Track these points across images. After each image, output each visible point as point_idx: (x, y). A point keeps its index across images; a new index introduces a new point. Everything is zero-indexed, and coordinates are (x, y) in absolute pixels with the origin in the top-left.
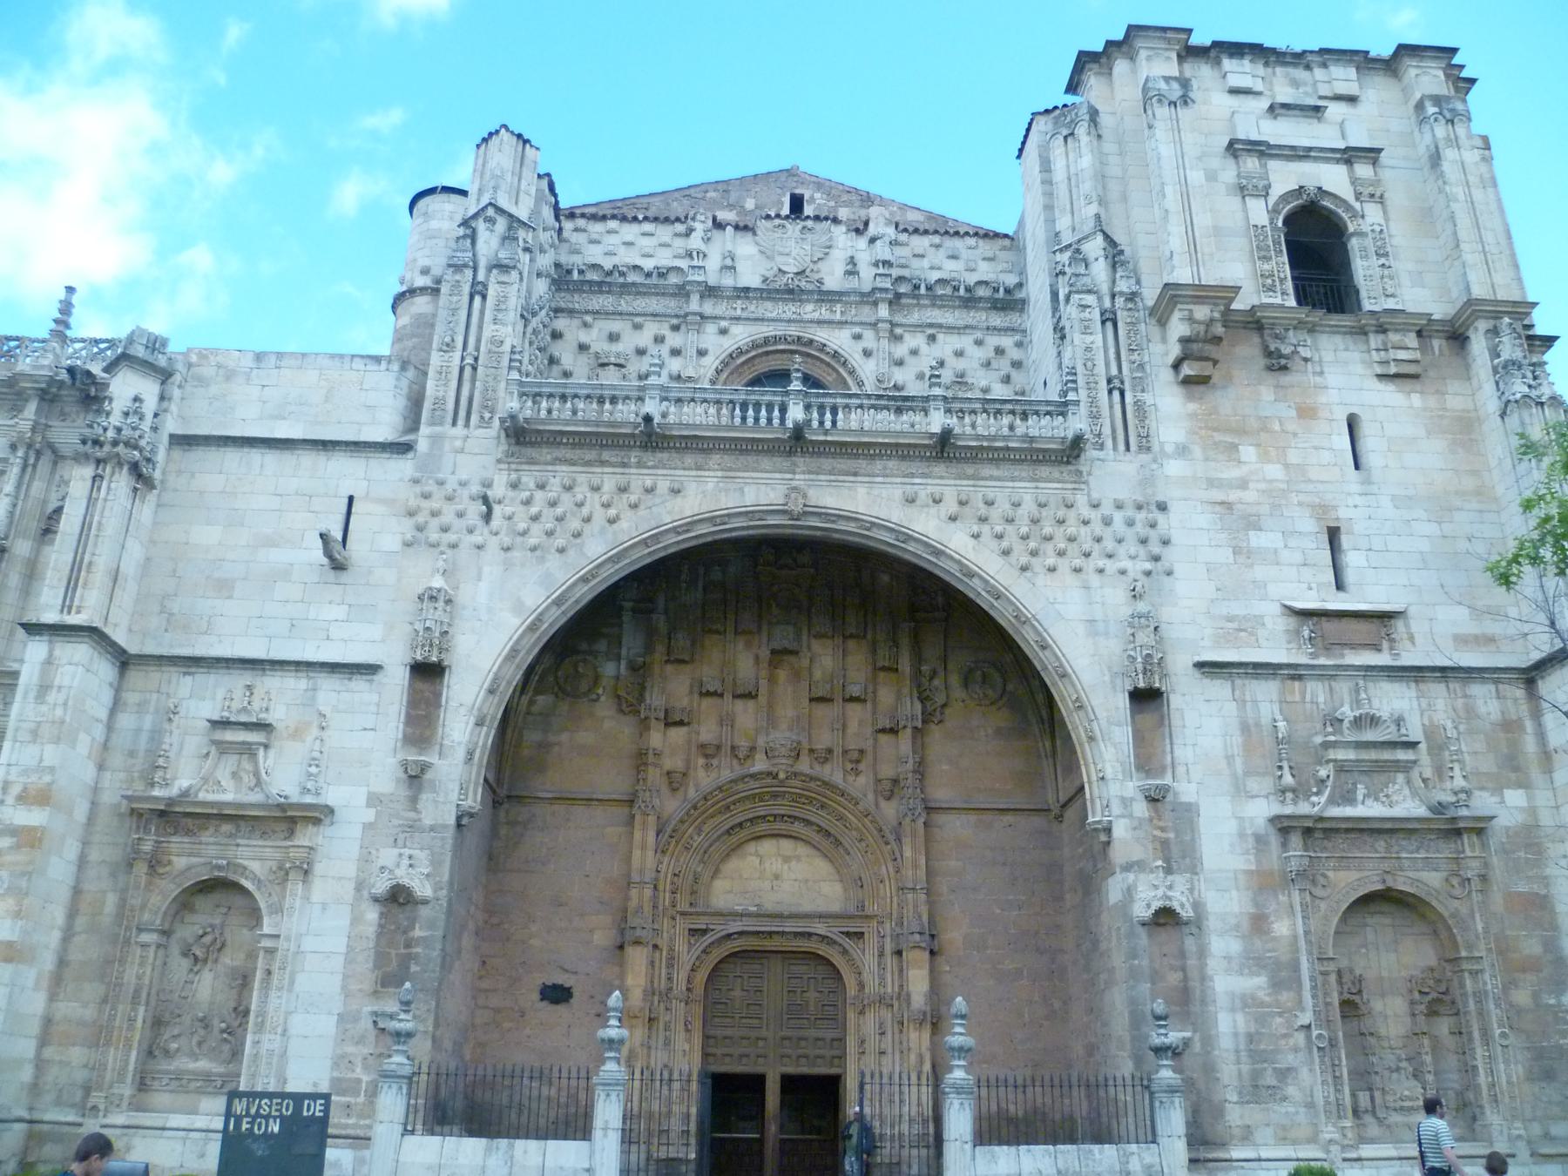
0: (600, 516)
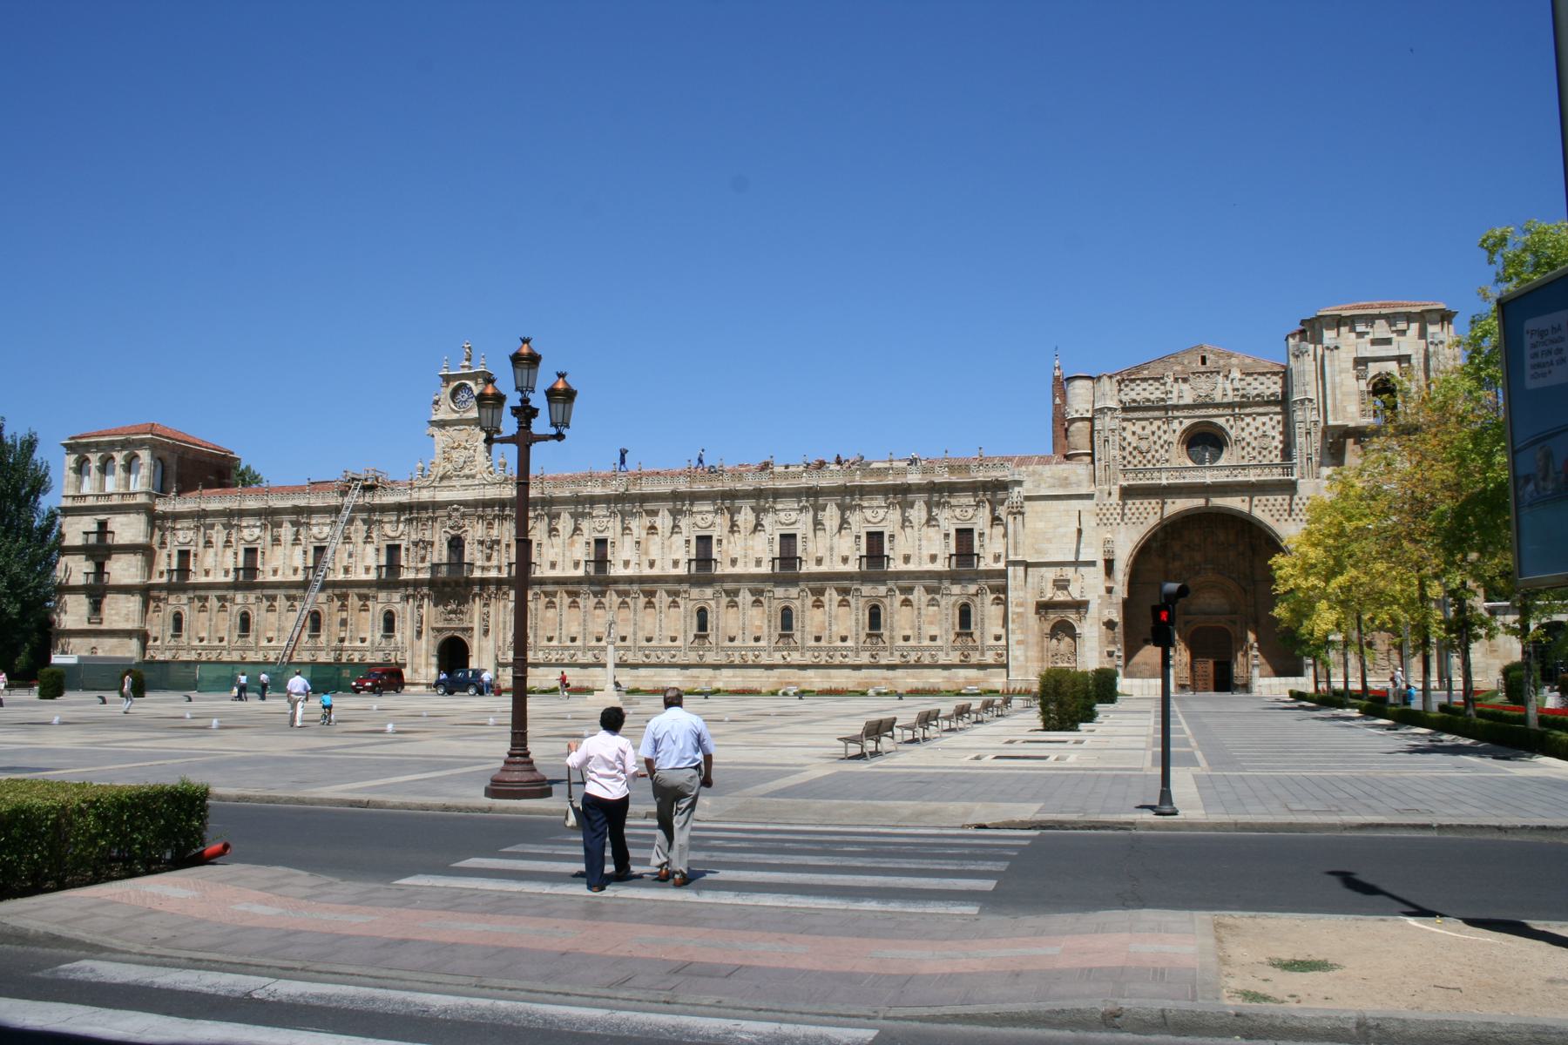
0: (1152, 512)
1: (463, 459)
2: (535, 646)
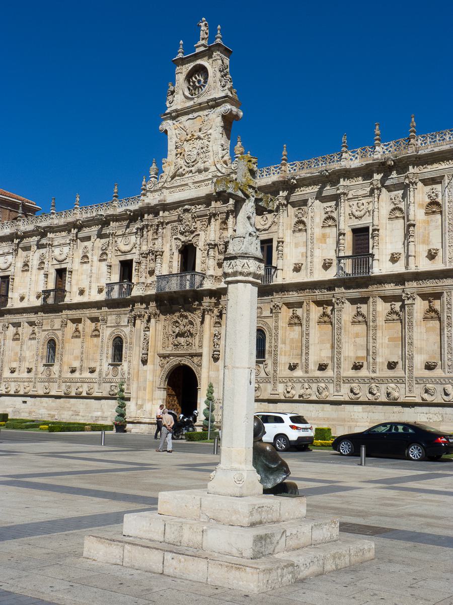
1: (195, 152)
2: (275, 377)
